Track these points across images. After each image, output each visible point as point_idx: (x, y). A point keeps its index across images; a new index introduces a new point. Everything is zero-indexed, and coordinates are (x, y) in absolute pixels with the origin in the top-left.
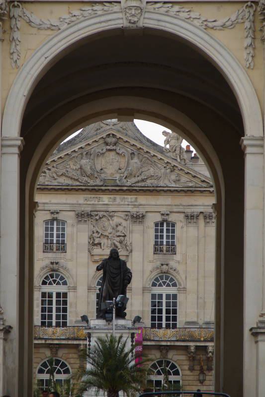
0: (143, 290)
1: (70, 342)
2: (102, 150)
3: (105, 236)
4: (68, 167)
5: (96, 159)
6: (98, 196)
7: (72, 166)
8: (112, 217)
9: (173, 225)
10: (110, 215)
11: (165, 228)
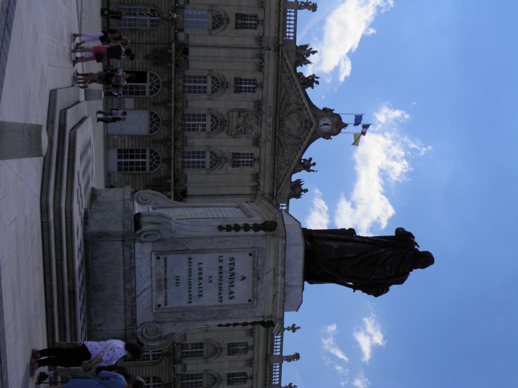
0: (208, 146)
1: (173, 96)
2: (302, 118)
3: (245, 120)
4: (292, 95)
5: (297, 114)
6: (272, 115)
7: (292, 98)
8: (258, 124)
9: (251, 165)
10: (259, 123)
11: (249, 160)
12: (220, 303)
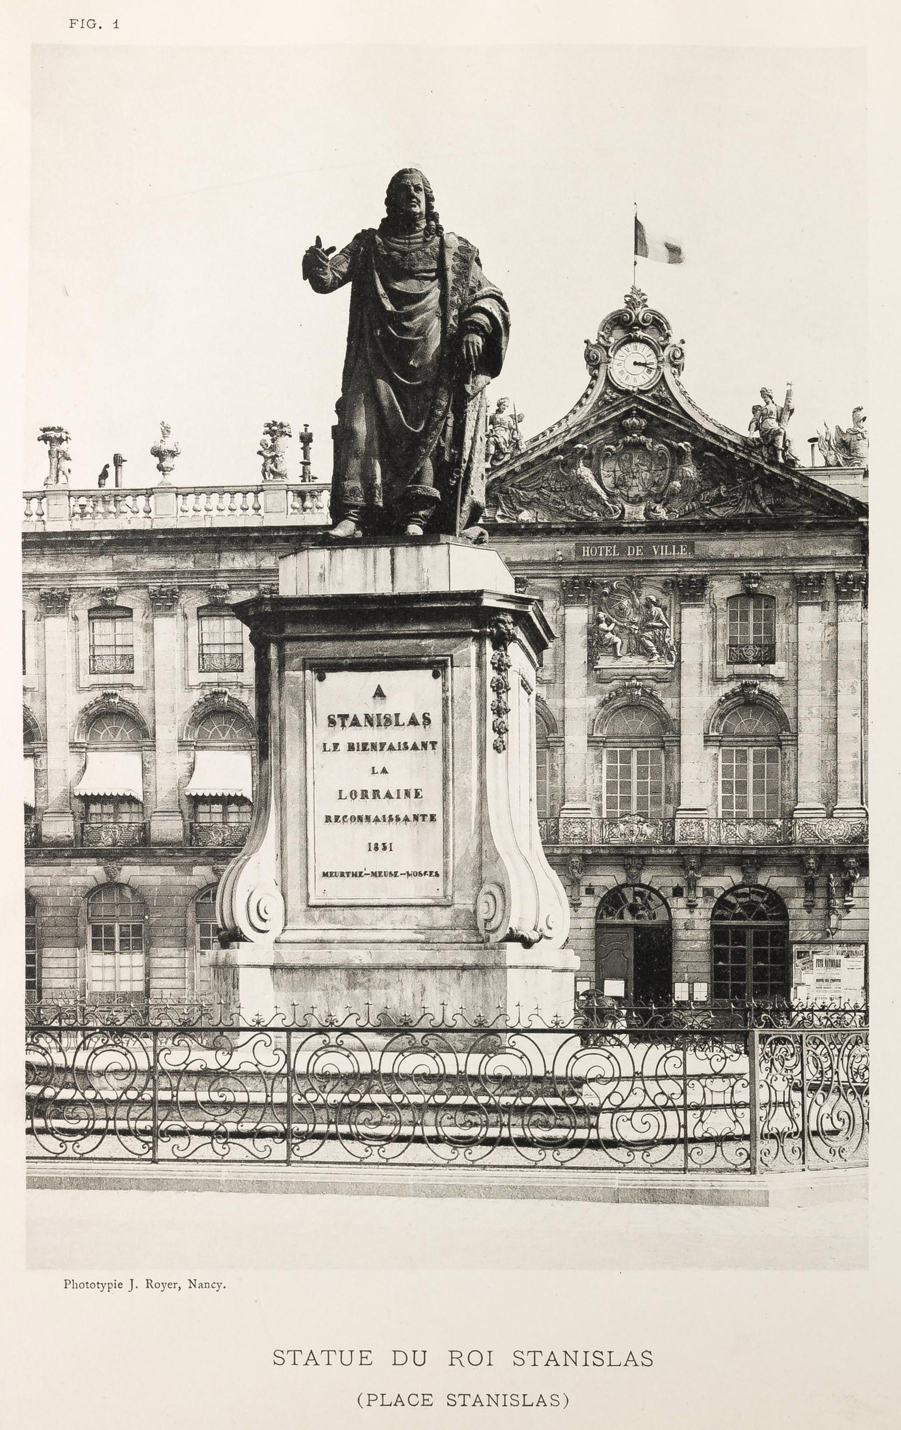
12: (439, 746)
